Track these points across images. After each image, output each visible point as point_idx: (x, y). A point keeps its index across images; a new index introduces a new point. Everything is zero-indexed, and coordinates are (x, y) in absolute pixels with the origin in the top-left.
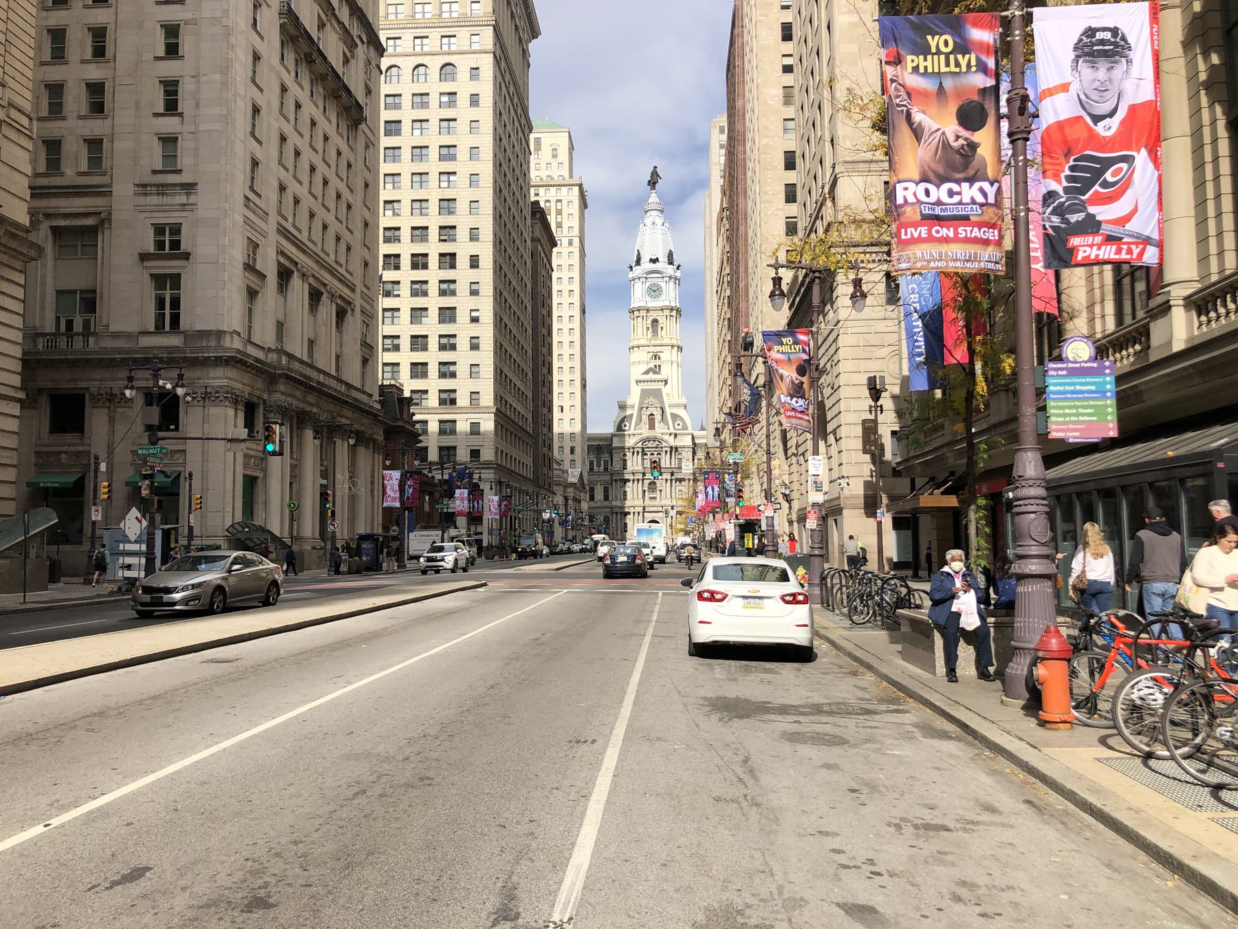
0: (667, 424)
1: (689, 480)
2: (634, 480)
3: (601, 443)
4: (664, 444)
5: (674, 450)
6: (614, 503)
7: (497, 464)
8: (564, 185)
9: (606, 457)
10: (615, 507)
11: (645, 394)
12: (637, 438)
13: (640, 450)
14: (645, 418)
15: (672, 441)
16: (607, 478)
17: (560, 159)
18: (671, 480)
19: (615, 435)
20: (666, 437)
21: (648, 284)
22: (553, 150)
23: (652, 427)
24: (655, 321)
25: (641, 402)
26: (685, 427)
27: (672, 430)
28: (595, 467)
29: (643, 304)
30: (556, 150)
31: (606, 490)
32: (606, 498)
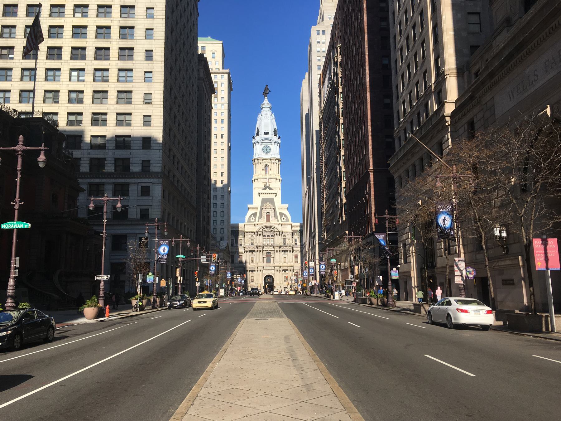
0: (276, 217)
1: (290, 251)
4: (276, 230)
5: (280, 233)
8: (219, 73)
11: (264, 201)
12: (260, 226)
13: (261, 233)
14: (264, 215)
15: (280, 228)
17: (217, 59)
20: (277, 226)
21: (263, 146)
22: (213, 53)
23: (268, 220)
25: (262, 205)
26: (287, 220)
27: (280, 222)
29: (260, 156)
30: (214, 53)
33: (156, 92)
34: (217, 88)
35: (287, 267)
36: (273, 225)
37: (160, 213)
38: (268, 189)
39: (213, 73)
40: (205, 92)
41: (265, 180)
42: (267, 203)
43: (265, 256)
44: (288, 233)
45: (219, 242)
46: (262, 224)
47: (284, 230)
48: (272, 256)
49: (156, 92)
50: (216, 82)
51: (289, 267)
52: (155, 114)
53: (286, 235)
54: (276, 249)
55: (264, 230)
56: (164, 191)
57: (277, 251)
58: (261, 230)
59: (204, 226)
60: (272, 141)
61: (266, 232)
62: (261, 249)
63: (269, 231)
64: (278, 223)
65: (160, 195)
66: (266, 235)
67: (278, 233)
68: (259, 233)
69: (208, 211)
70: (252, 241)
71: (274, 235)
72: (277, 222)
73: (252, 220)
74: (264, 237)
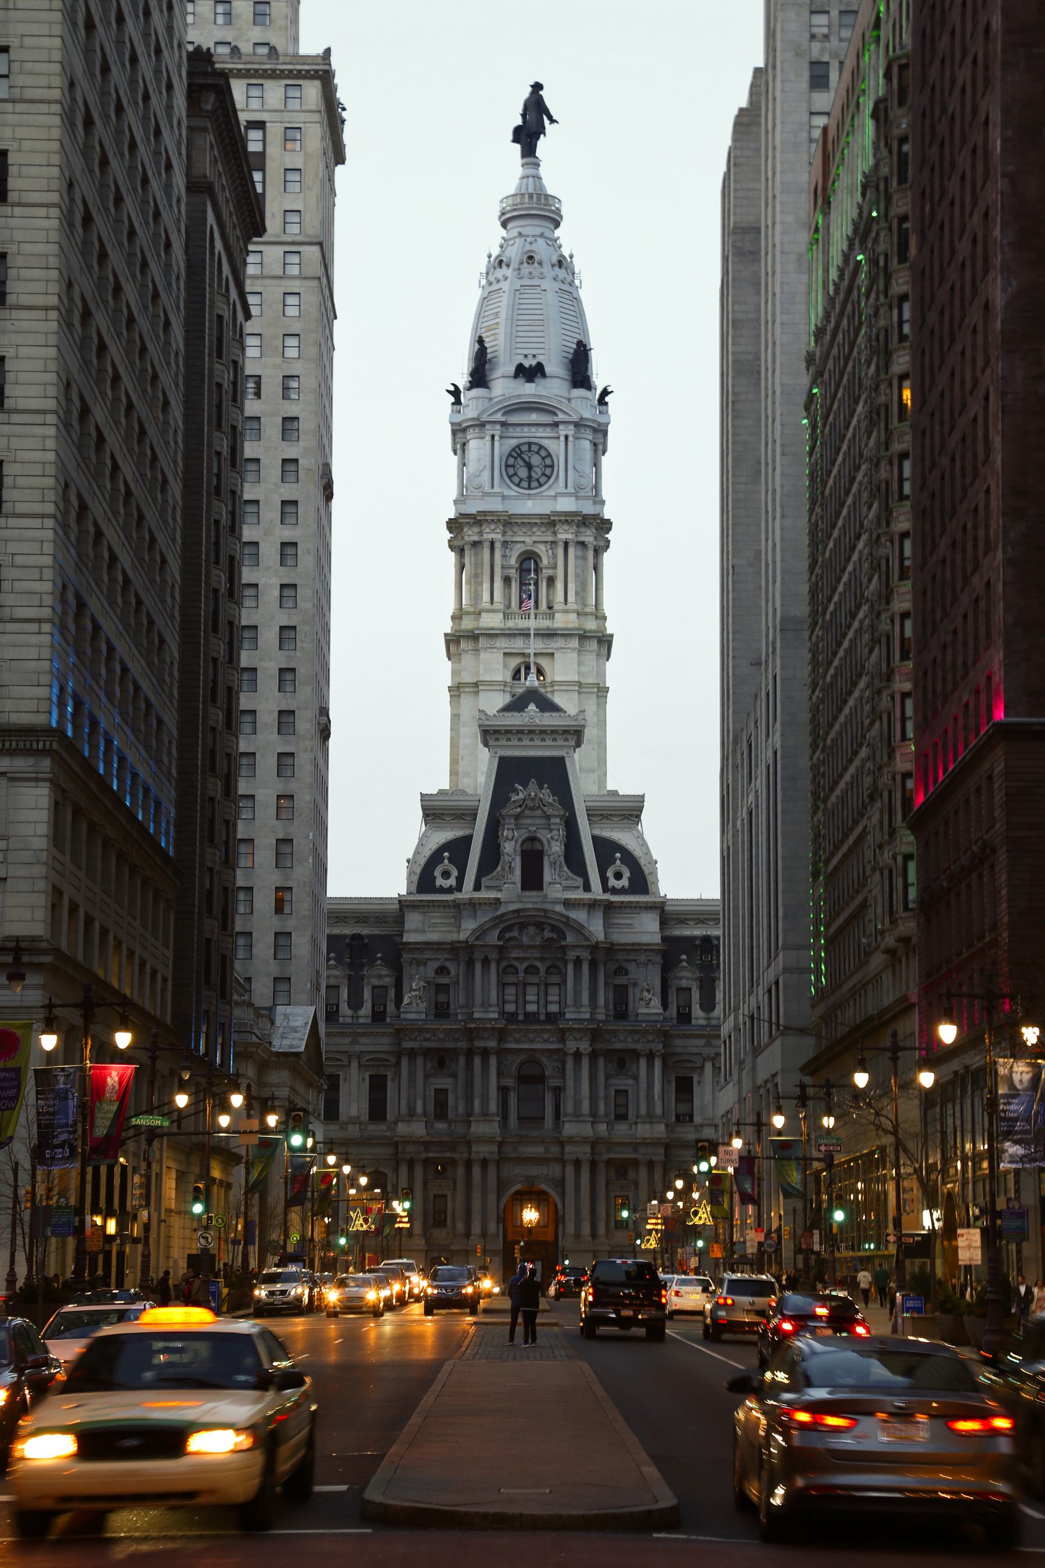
1: (650, 1056)
2: (470, 1054)
3: (365, 931)
4: (570, 938)
6: (402, 1129)
7: (57, 952)
9: (379, 975)
10: (408, 1141)
12: (484, 917)
15: (596, 928)
16: (383, 1044)
18: (594, 1056)
19: (415, 906)
20: (579, 916)
23: (532, 880)
24: (529, 558)
28: (345, 1009)
29: (495, 505)
31: (378, 1087)
32: (377, 1110)
33: (24, 351)
34: (262, 155)
35: (635, 1146)
36: (559, 908)
37: (41, 914)
38: (532, 707)
39: (241, 74)
40: (219, 245)
41: (518, 644)
42: (525, 786)
43: (510, 1082)
44: (643, 958)
45: (271, 1010)
46: (498, 901)
47: (622, 937)
48: (553, 1082)
49: (24, 351)
50: (260, 125)
51: (642, 1149)
52: (22, 456)
53: (632, 967)
54: (571, 1046)
55: (508, 935)
56: (57, 807)
57: (578, 1055)
58: (493, 938)
59: (208, 941)
60: (561, 417)
61: (521, 947)
62: (493, 1044)
63: (538, 941)
64: (587, 896)
65: (43, 829)
66: (521, 967)
67: (585, 955)
68: (478, 955)
69: (226, 861)
70: (442, 998)
71: (560, 965)
72: (580, 895)
73: (440, 882)
74: (510, 979)
